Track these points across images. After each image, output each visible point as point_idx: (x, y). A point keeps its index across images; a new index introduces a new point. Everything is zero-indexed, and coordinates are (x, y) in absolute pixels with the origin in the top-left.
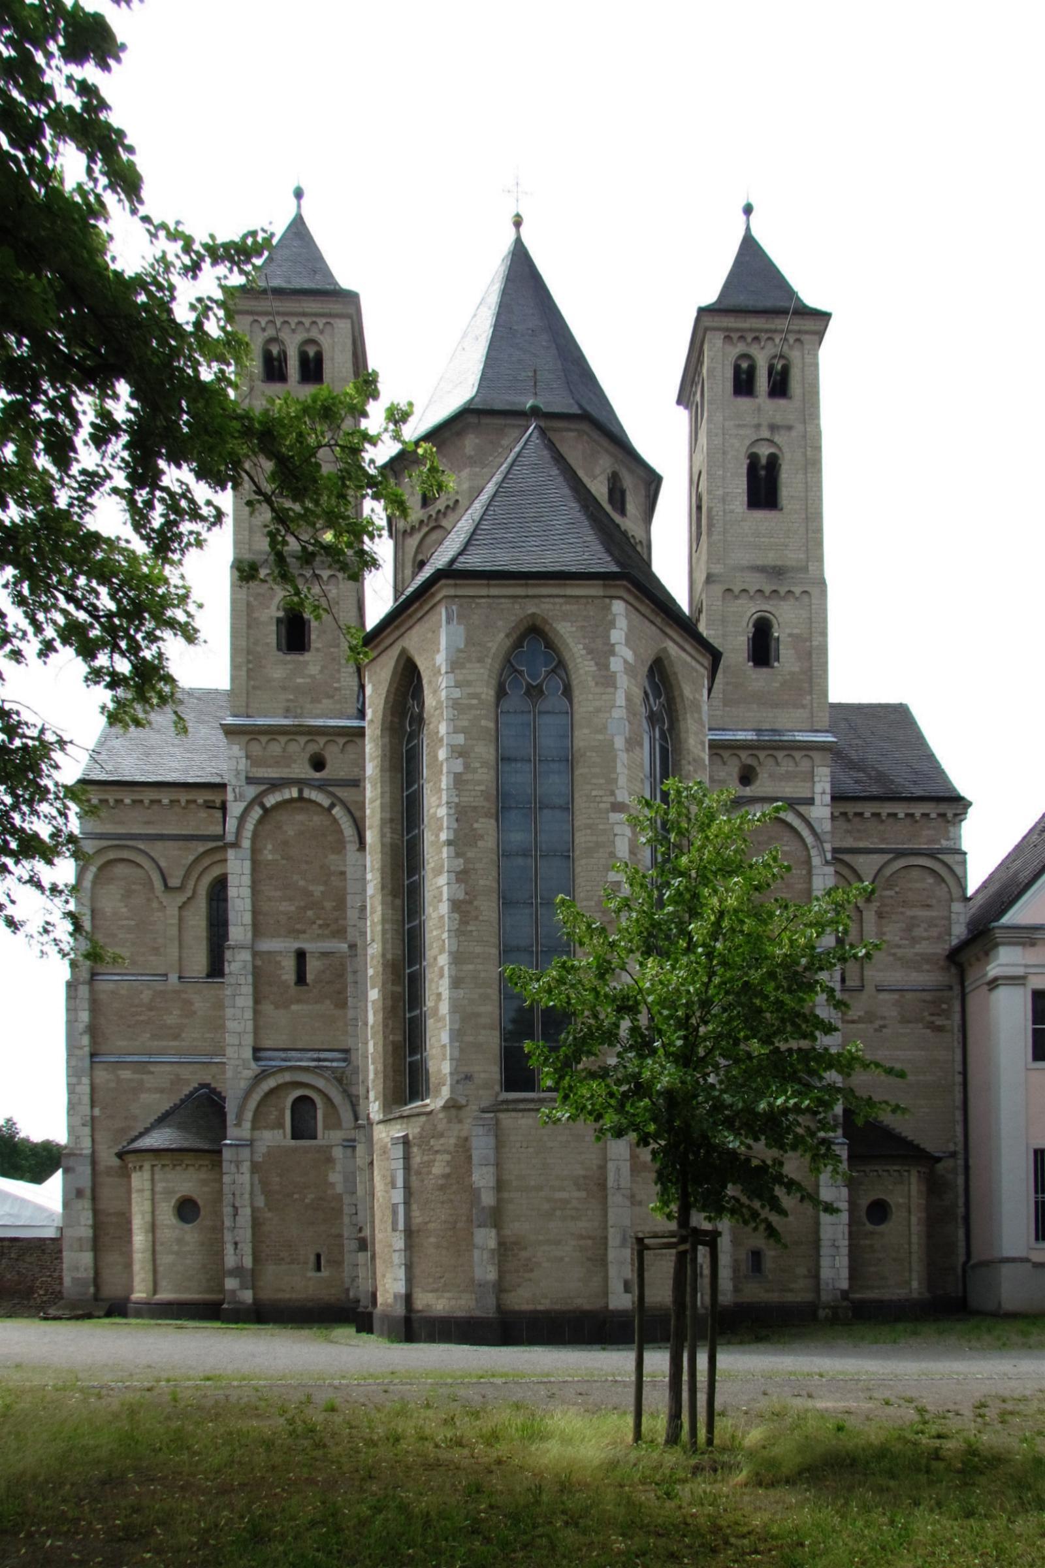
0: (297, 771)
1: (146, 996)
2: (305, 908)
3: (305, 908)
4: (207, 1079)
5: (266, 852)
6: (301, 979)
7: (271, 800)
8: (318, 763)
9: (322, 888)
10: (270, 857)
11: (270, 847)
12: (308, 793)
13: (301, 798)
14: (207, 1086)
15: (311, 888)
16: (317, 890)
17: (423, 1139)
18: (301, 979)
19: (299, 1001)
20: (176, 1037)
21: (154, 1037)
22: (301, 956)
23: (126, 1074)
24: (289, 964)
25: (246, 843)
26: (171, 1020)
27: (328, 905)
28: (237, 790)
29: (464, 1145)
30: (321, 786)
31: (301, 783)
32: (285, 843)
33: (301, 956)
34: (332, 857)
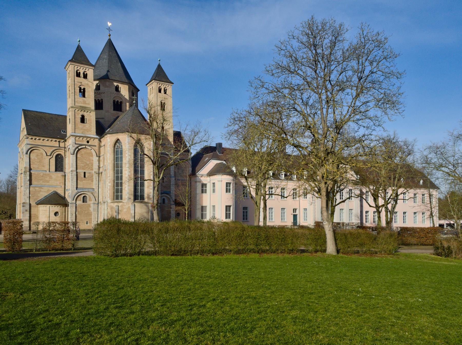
1: (42, 174)
4: (55, 190)
6: (85, 176)
8: (88, 142)
13: (85, 148)
14: (55, 191)
16: (88, 162)
17: (122, 206)
18: (85, 176)
19: (84, 180)
20: (48, 182)
21: (43, 182)
22: (85, 173)
23: (37, 189)
24: (83, 174)
26: (48, 179)
27: (90, 165)
29: (129, 207)
30: (90, 146)
32: (82, 154)
33: (85, 173)
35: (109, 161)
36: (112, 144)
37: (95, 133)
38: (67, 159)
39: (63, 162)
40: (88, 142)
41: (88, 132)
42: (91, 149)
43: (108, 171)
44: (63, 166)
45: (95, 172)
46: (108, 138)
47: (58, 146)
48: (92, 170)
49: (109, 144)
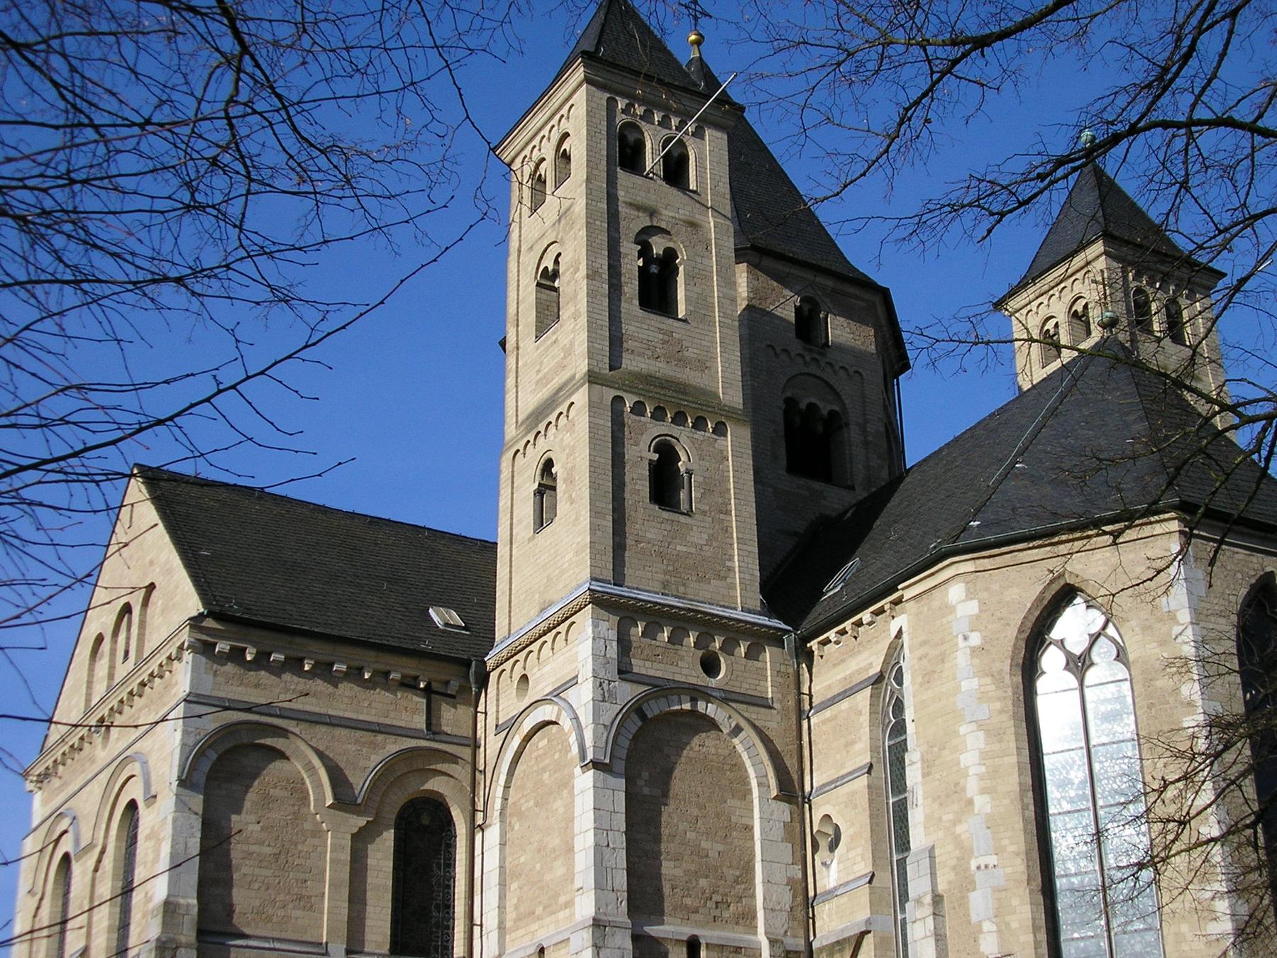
0: (685, 671)
2: (697, 875)
3: (697, 875)
5: (641, 783)
7: (653, 710)
8: (710, 666)
9: (720, 847)
10: (646, 791)
11: (645, 775)
12: (701, 706)
15: (704, 844)
25: (620, 766)
28: (605, 686)
31: (697, 693)
34: (730, 802)
35: (982, 804)
36: (1012, 632)
37: (756, 599)
38: (492, 835)
39: (450, 864)
40: (710, 666)
41: (703, 579)
42: (737, 730)
43: (979, 903)
44: (448, 907)
45: (773, 942)
46: (956, 592)
47: (420, 722)
48: (748, 918)
49: (976, 639)
